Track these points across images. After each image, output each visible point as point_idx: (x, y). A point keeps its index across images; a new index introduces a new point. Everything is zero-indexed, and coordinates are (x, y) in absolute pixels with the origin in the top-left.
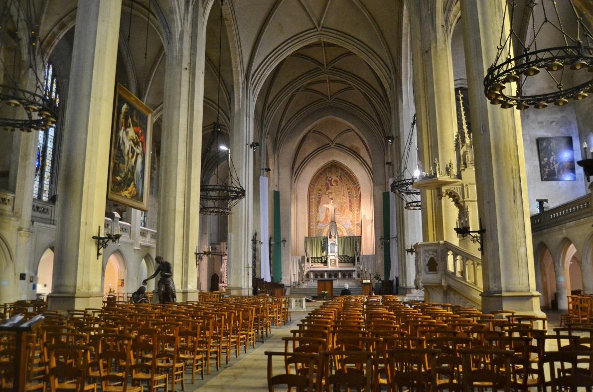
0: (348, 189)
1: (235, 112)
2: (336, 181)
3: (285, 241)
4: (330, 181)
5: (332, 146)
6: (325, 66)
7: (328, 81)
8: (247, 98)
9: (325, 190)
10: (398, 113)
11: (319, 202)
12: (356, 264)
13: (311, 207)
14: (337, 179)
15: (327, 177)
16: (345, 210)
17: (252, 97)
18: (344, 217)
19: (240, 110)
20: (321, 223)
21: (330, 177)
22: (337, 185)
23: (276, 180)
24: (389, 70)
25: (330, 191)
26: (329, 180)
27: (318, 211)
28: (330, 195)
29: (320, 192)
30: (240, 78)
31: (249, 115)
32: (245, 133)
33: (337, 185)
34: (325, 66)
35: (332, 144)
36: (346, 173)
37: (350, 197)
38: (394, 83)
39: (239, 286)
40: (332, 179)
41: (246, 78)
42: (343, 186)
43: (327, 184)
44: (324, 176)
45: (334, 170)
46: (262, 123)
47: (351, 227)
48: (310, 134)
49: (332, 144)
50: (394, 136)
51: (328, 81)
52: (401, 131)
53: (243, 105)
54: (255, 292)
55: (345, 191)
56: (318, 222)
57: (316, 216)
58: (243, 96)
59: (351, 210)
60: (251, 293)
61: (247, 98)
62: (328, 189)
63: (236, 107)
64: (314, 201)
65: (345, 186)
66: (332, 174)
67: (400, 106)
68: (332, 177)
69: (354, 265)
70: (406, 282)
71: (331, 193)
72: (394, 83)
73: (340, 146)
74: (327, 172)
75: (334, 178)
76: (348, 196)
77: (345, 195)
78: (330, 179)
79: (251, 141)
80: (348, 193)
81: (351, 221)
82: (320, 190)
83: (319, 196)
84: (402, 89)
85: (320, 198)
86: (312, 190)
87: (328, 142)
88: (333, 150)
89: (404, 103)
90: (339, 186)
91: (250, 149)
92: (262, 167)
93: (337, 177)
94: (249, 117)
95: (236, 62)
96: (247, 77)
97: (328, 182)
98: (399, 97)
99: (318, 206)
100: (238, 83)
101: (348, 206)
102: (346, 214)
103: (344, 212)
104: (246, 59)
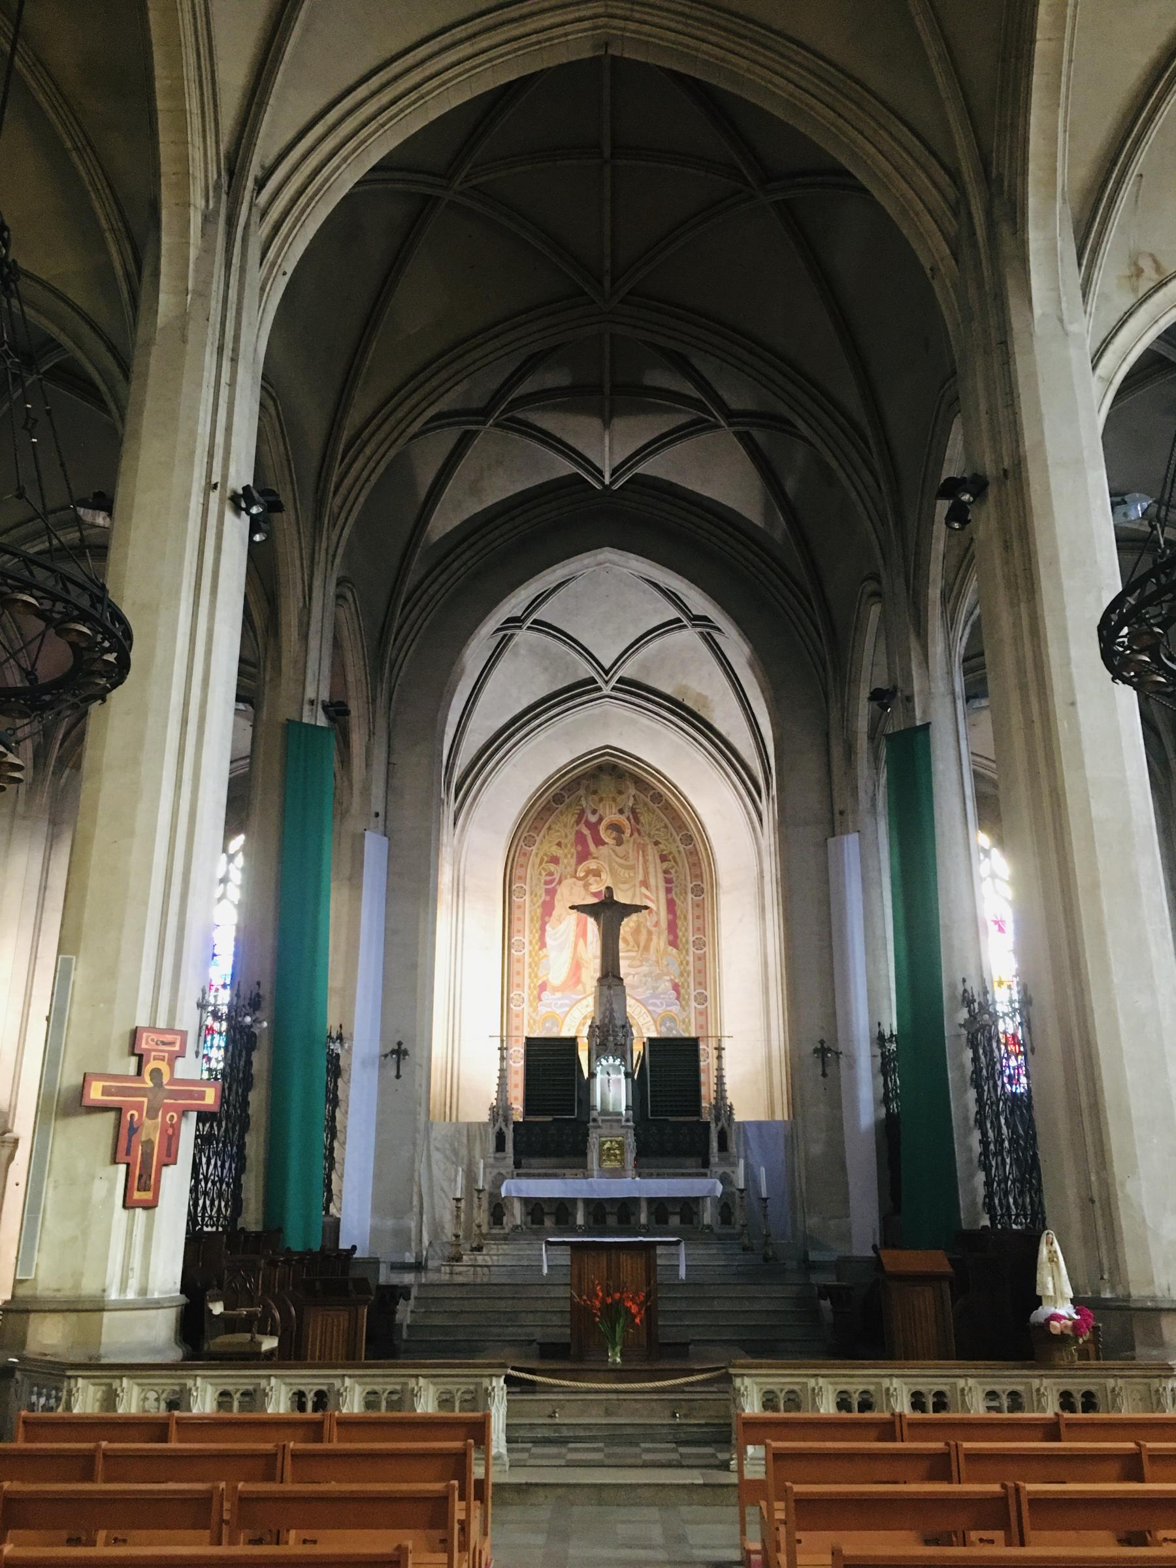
0: (663, 858)
1: (161, 320)
2: (616, 828)
3: (406, 1053)
4: (594, 828)
5: (607, 690)
6: (607, 284)
7: (607, 390)
8: (228, 265)
9: (573, 861)
10: (1007, 360)
11: (548, 908)
12: (715, 1158)
13: (516, 925)
14: (622, 819)
15: (583, 812)
16: (649, 940)
17: (255, 275)
18: (645, 969)
19: (183, 319)
20: (556, 989)
21: (594, 812)
22: (619, 842)
23: (378, 790)
24: (954, 175)
25: (592, 864)
26: (589, 825)
27: (543, 945)
28: (591, 879)
29: (552, 867)
30: (196, 154)
31: (235, 350)
32: (203, 429)
33: (619, 842)
34: (607, 284)
35: (607, 682)
36: (658, 797)
37: (668, 891)
38: (981, 233)
39: (89, 1287)
40: (601, 819)
41: (231, 173)
42: (645, 845)
43: (580, 839)
44: (569, 806)
45: (607, 784)
46: (320, 503)
47: (675, 1009)
48: (523, 636)
49: (607, 682)
50: (989, 468)
51: (607, 390)
52: (1028, 442)
53: (203, 294)
54: (192, 1326)
55: (651, 870)
56: (543, 987)
57: (534, 965)
58: (207, 250)
59: (673, 943)
60: (156, 1331)
61: (228, 265)
62: (583, 856)
63: (163, 297)
64: (528, 904)
65: (650, 849)
66: (601, 800)
67: (1016, 323)
68: (601, 812)
69: (706, 1164)
70: (1117, 1267)
71: (597, 873)
72: (981, 233)
73: (635, 690)
74: (582, 792)
75: (611, 815)
76: (662, 884)
77: (652, 881)
78: (593, 819)
79: (241, 475)
80: (661, 876)
81: (676, 987)
82: (555, 860)
83: (546, 883)
84: (1023, 244)
85: (551, 893)
86: (522, 860)
87: (586, 670)
88: (609, 706)
89: (1038, 311)
90: (628, 847)
91: (229, 515)
92: (310, 694)
93: (621, 811)
94: (234, 360)
95: (176, 62)
96: (234, 166)
97: (586, 832)
98: (1011, 283)
99: (543, 930)
100: (183, 184)
101: (664, 924)
102: (652, 956)
103: (647, 948)
104: (234, 75)
